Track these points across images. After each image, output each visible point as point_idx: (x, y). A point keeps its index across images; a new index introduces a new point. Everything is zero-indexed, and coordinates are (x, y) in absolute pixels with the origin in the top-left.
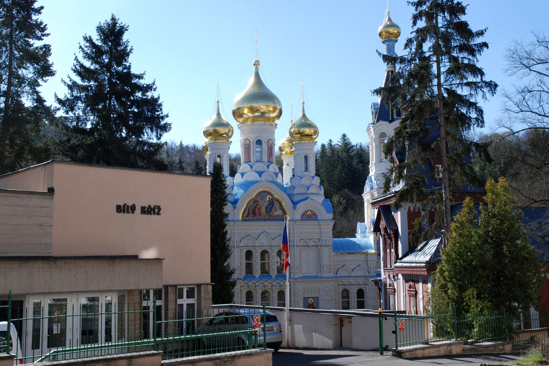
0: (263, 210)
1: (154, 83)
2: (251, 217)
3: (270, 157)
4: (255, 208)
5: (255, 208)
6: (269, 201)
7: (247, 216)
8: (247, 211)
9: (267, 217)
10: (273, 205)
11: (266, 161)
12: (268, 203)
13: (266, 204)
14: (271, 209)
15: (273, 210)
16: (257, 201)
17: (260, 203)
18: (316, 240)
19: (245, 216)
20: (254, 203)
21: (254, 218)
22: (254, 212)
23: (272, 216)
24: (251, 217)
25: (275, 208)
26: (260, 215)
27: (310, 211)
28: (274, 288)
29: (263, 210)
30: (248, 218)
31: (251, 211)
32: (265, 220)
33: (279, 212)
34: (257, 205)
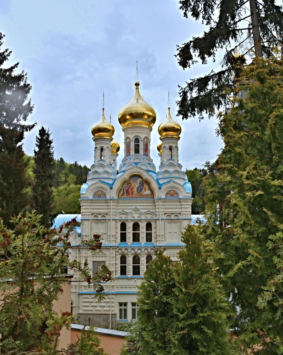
0: (135, 190)
1: (23, 72)
2: (125, 196)
3: (145, 152)
4: (129, 188)
5: (129, 188)
6: (140, 183)
7: (122, 195)
8: (122, 191)
9: (138, 196)
10: (143, 187)
11: (143, 154)
12: (139, 185)
13: (137, 186)
14: (141, 189)
15: (143, 190)
16: (130, 183)
17: (133, 184)
18: (179, 215)
19: (121, 195)
20: (128, 184)
21: (128, 197)
22: (127, 192)
23: (142, 195)
24: (125, 196)
25: (145, 188)
26: (132, 193)
27: (173, 190)
28: (143, 253)
29: (135, 190)
30: (122, 197)
31: (125, 191)
32: (136, 197)
33: (148, 192)
34: (130, 186)
